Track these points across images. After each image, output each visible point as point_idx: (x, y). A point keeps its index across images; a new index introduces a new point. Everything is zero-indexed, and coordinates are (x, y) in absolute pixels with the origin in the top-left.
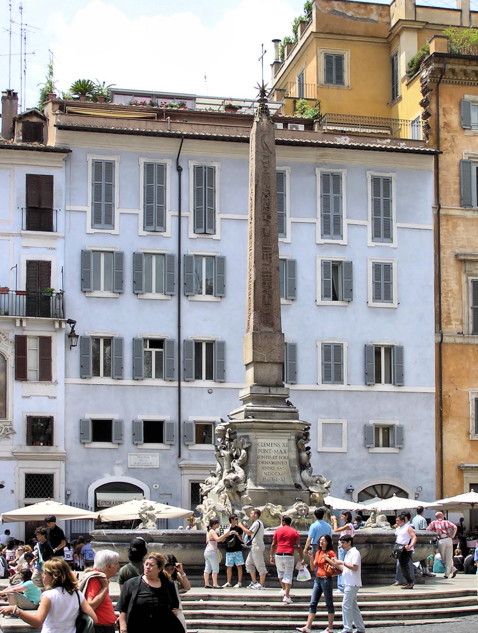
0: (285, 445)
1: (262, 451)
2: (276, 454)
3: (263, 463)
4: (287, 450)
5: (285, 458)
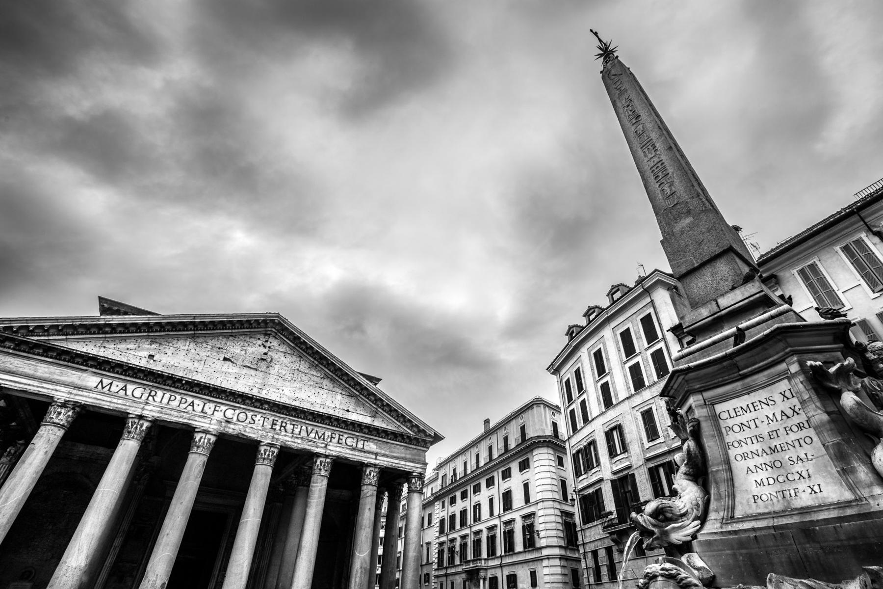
0: (788, 394)
1: (736, 428)
2: (774, 426)
3: (744, 456)
4: (798, 406)
5: (800, 427)
